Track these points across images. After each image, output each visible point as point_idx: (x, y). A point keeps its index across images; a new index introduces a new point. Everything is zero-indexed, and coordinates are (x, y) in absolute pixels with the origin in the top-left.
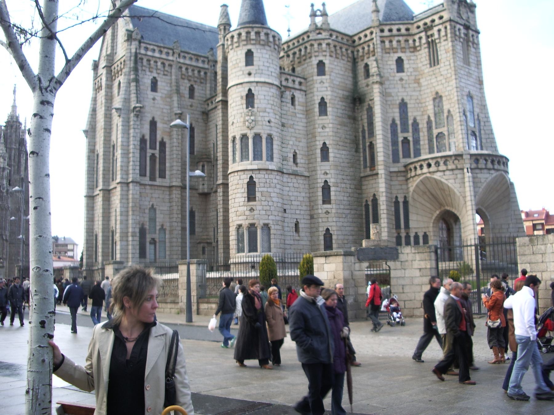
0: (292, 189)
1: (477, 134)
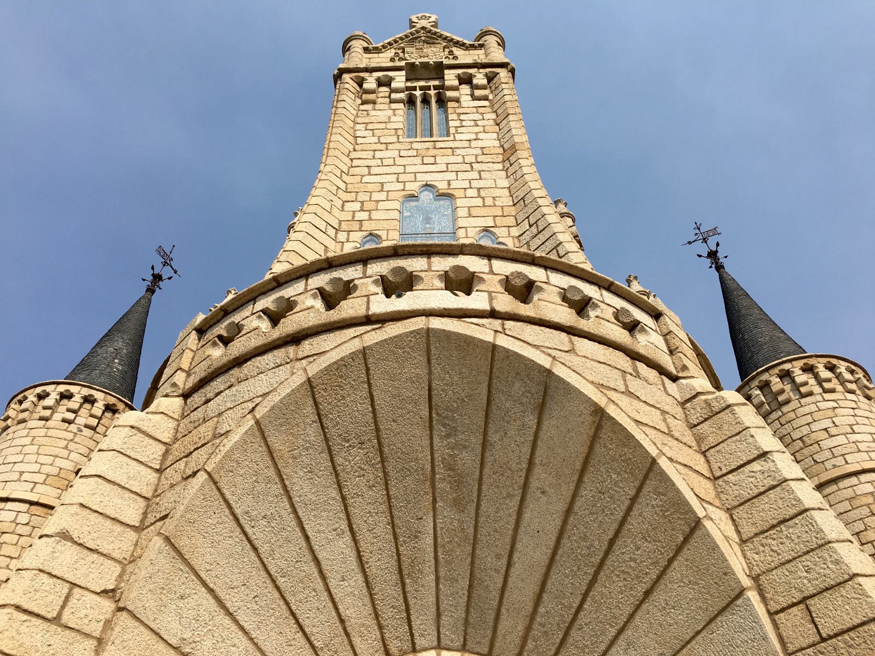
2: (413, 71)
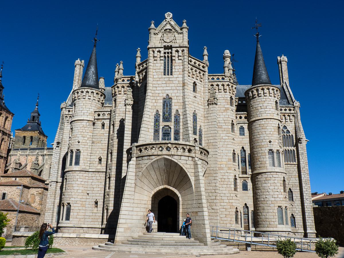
0: (96, 181)
1: (172, 127)
2: (165, 48)
